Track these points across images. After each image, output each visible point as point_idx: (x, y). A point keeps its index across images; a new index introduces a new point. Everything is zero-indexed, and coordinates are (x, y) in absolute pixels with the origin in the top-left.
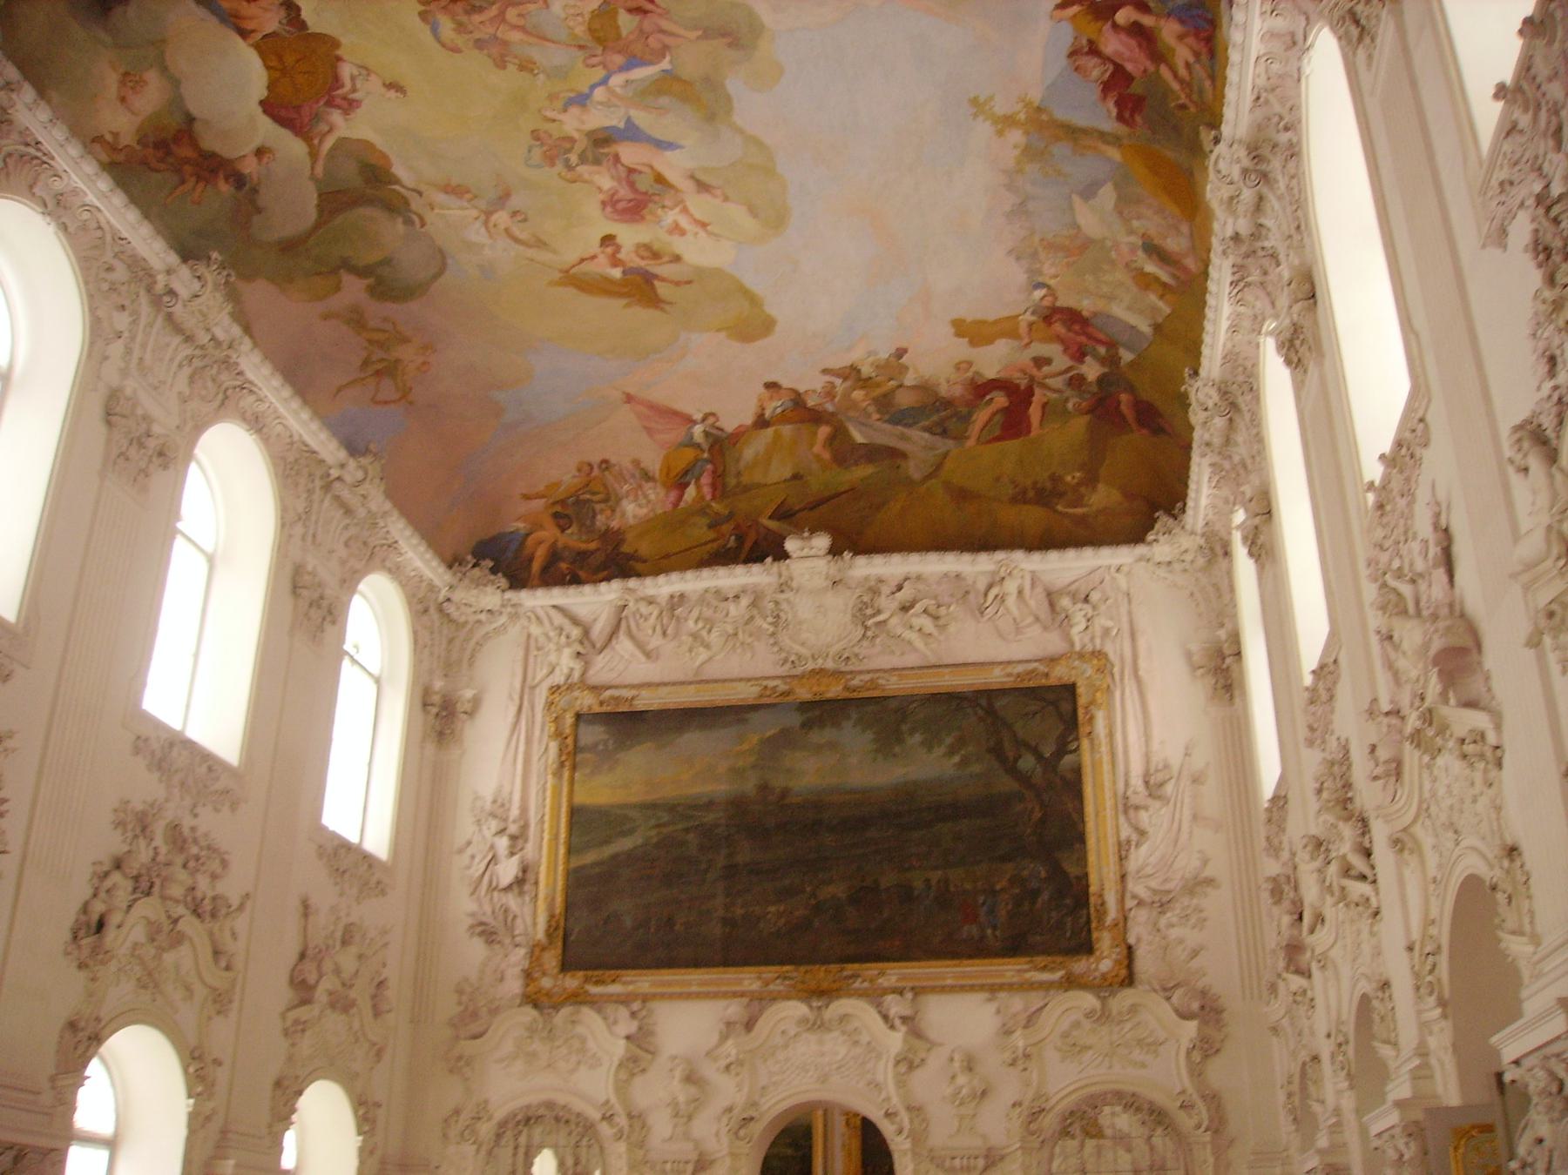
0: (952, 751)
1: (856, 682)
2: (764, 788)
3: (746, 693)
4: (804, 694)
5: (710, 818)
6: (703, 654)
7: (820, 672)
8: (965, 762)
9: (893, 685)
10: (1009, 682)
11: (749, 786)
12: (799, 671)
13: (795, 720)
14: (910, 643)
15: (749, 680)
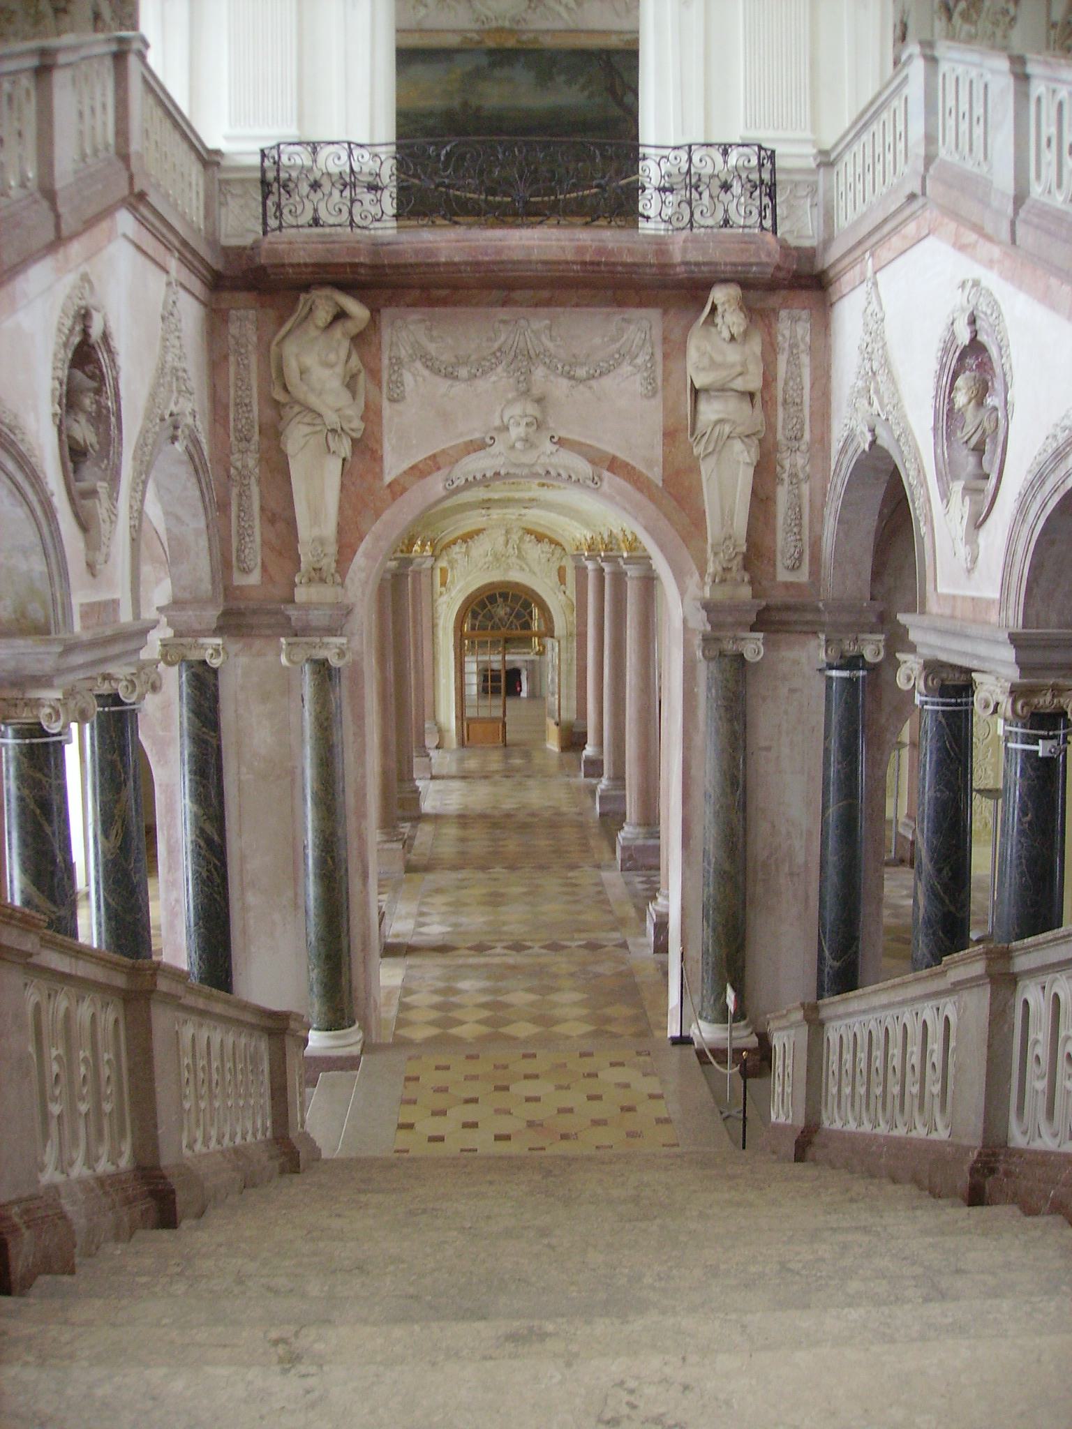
0: (583, 88)
1: (524, 38)
2: (465, 104)
3: (453, 41)
4: (491, 43)
5: (431, 122)
6: (423, 11)
7: (500, 30)
8: (591, 96)
9: (548, 42)
10: (621, 45)
11: (456, 103)
12: (487, 27)
13: (484, 61)
14: (559, 14)
15: (454, 31)
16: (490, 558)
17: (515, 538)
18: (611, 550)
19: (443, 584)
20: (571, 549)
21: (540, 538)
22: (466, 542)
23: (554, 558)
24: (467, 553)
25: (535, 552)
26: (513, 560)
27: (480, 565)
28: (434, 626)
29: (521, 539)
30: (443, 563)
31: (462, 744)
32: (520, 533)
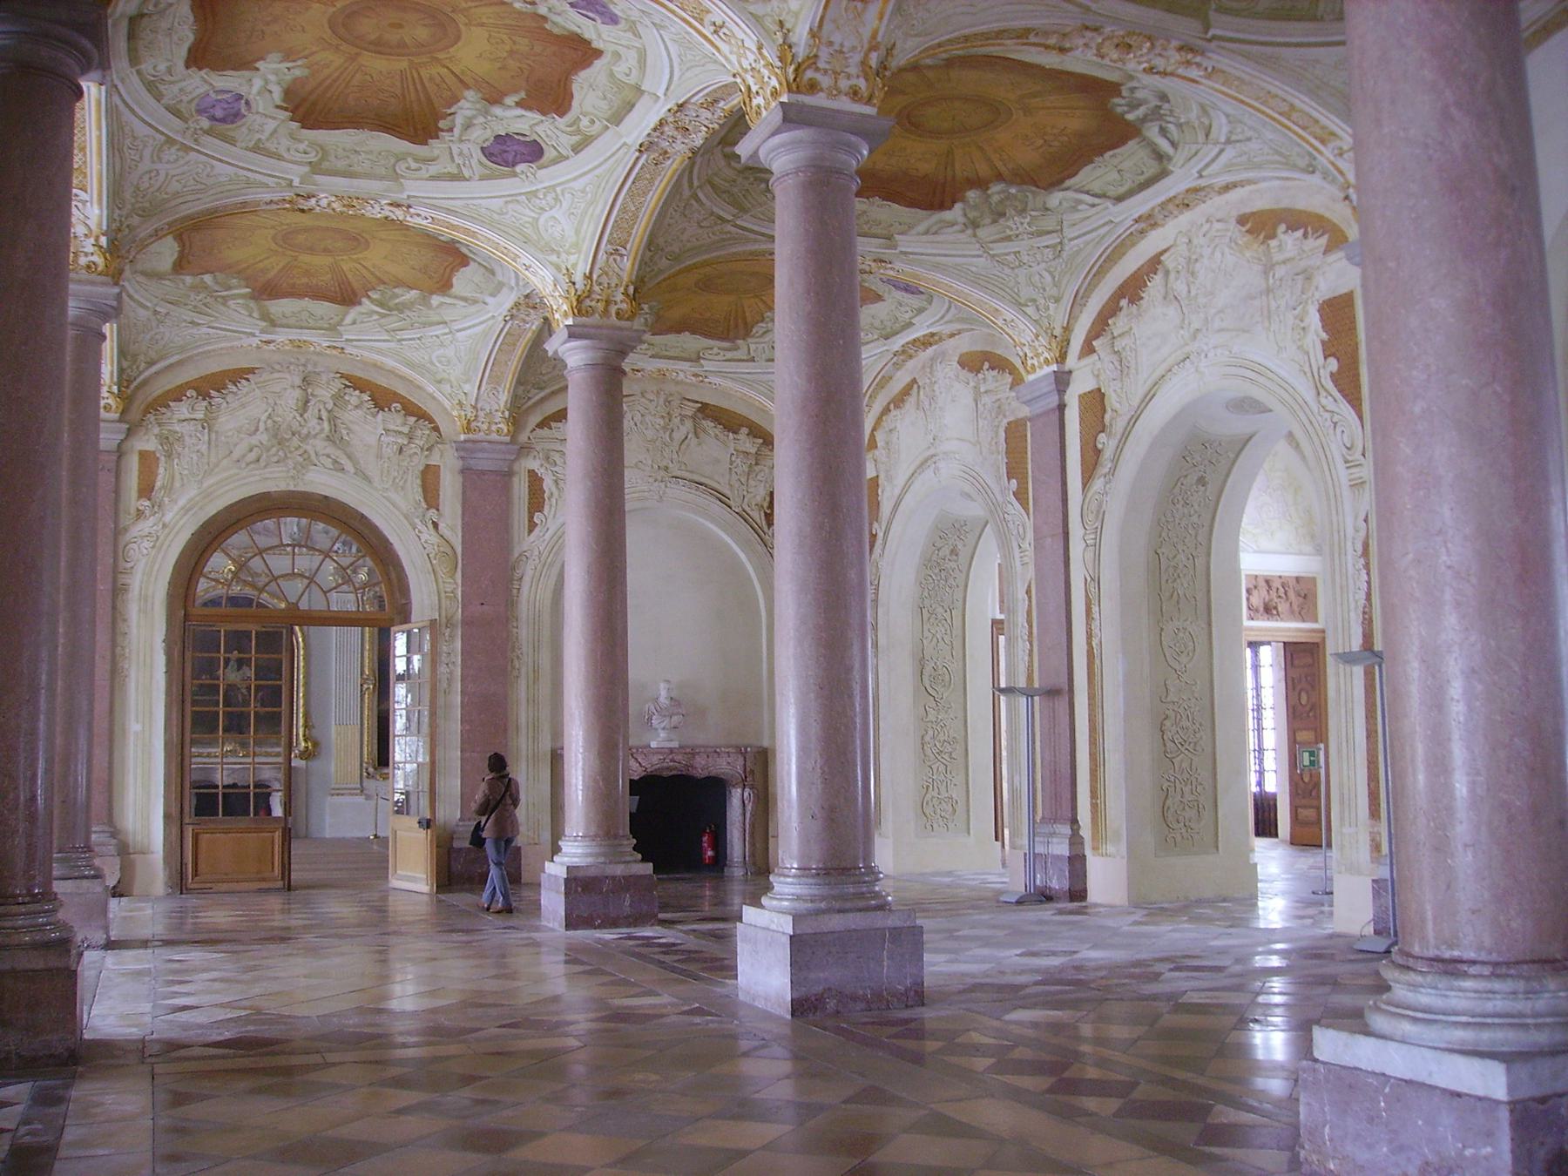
16: (263, 437)
17: (324, 393)
18: (813, 87)
19: (146, 490)
20: (452, 427)
21: (382, 399)
22: (206, 396)
23: (413, 448)
24: (207, 423)
25: (370, 430)
26: (320, 444)
27: (236, 455)
28: (118, 591)
29: (338, 398)
30: (147, 442)
31: (180, 883)
32: (338, 384)
